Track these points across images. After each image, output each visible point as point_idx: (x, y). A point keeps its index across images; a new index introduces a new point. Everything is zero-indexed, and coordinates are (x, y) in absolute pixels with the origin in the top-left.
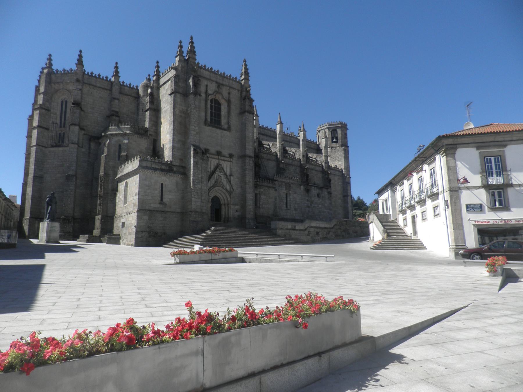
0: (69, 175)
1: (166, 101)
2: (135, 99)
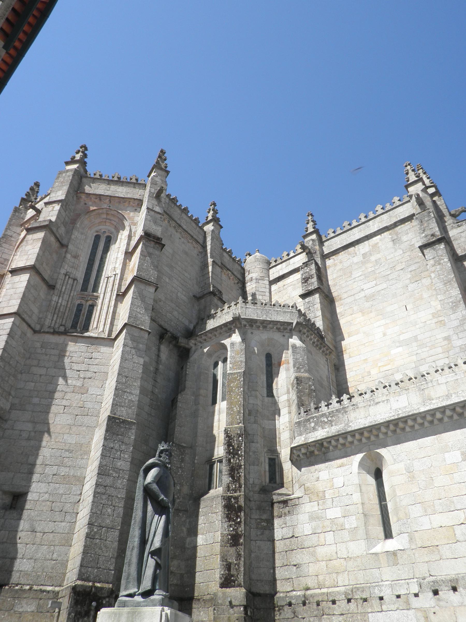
0: (119, 419)
1: (366, 277)
2: (238, 283)
